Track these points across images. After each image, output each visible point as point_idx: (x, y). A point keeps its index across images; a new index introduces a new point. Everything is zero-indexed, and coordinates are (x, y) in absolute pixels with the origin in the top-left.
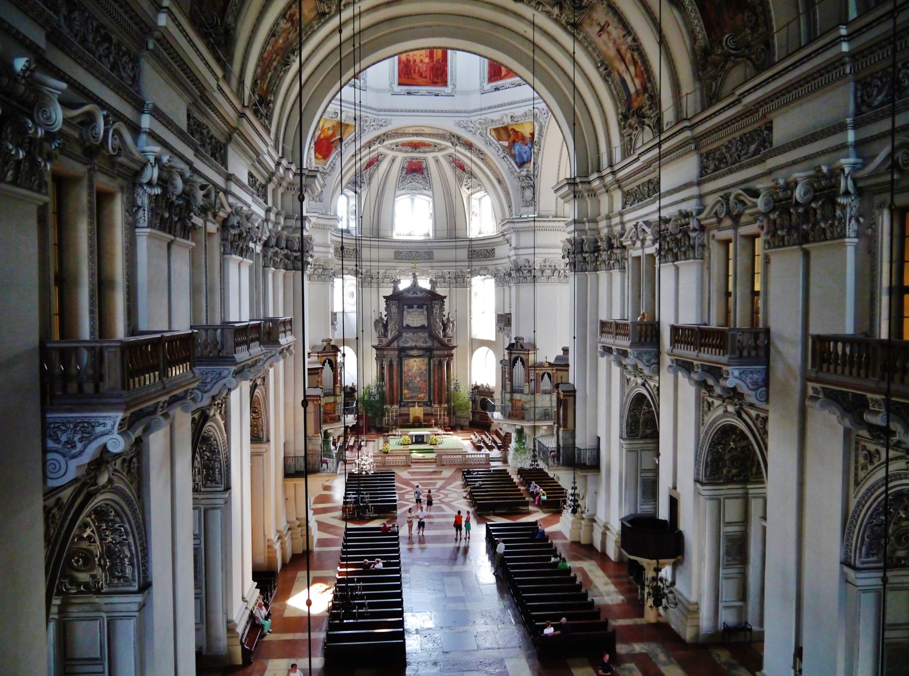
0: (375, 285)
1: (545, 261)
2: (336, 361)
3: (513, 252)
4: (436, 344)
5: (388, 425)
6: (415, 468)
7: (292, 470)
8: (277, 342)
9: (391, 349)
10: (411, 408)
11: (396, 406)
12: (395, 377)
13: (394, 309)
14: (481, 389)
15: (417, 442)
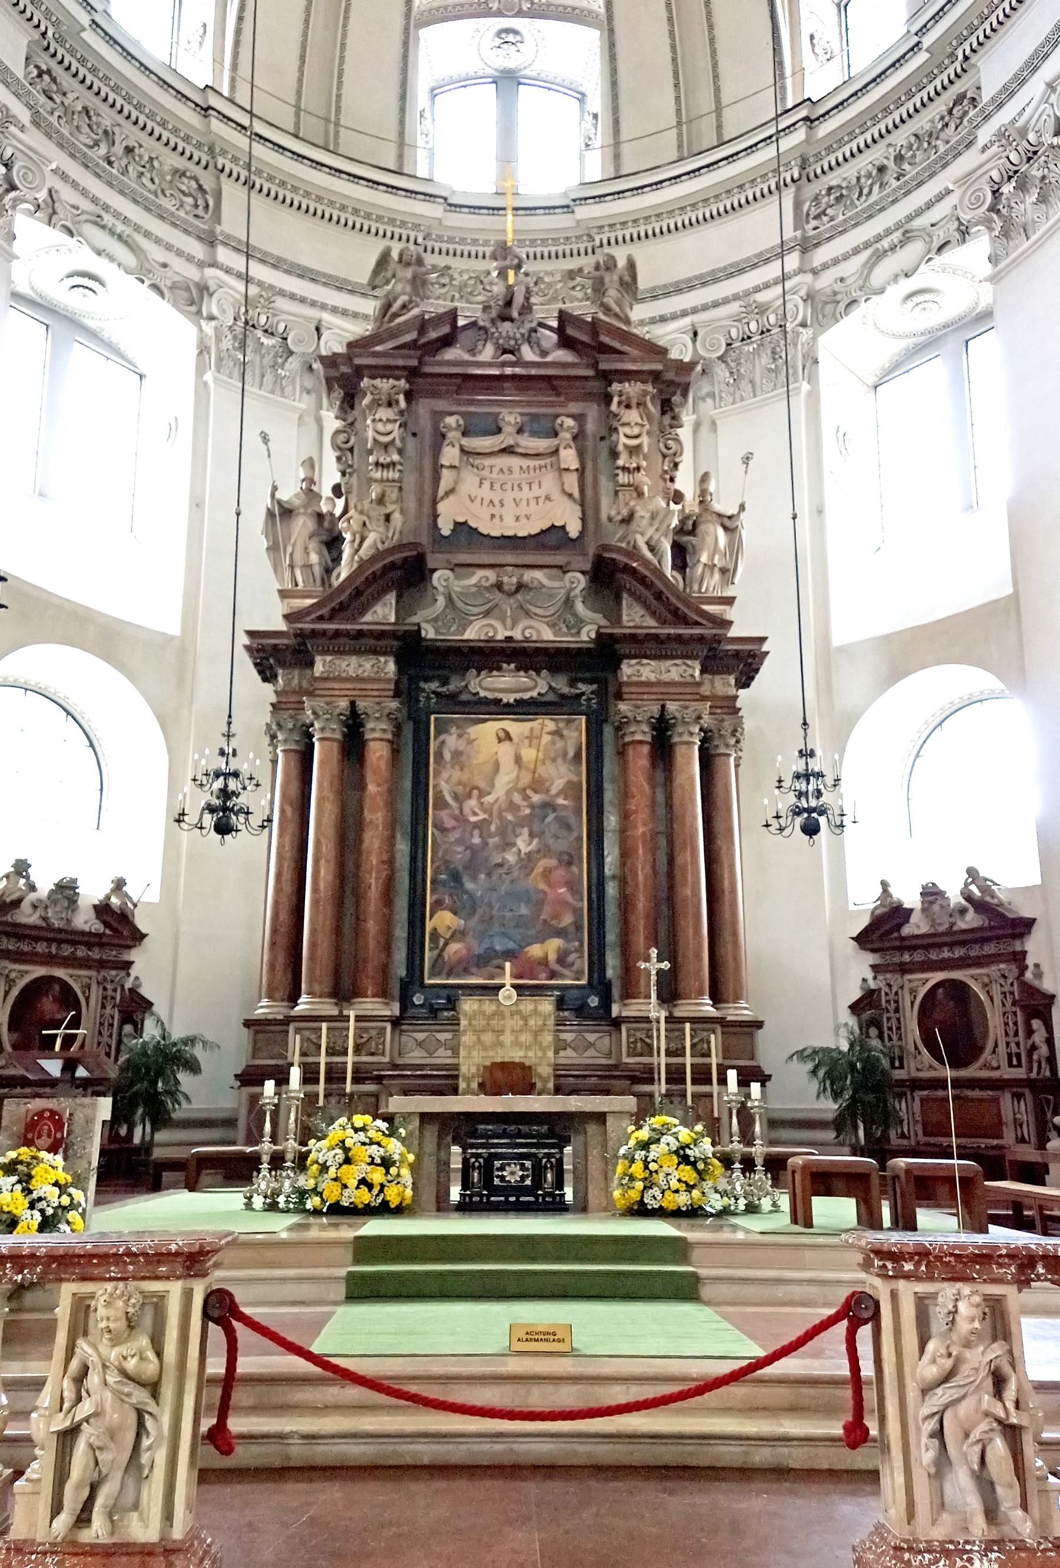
12: (375, 816)
14: (917, 926)
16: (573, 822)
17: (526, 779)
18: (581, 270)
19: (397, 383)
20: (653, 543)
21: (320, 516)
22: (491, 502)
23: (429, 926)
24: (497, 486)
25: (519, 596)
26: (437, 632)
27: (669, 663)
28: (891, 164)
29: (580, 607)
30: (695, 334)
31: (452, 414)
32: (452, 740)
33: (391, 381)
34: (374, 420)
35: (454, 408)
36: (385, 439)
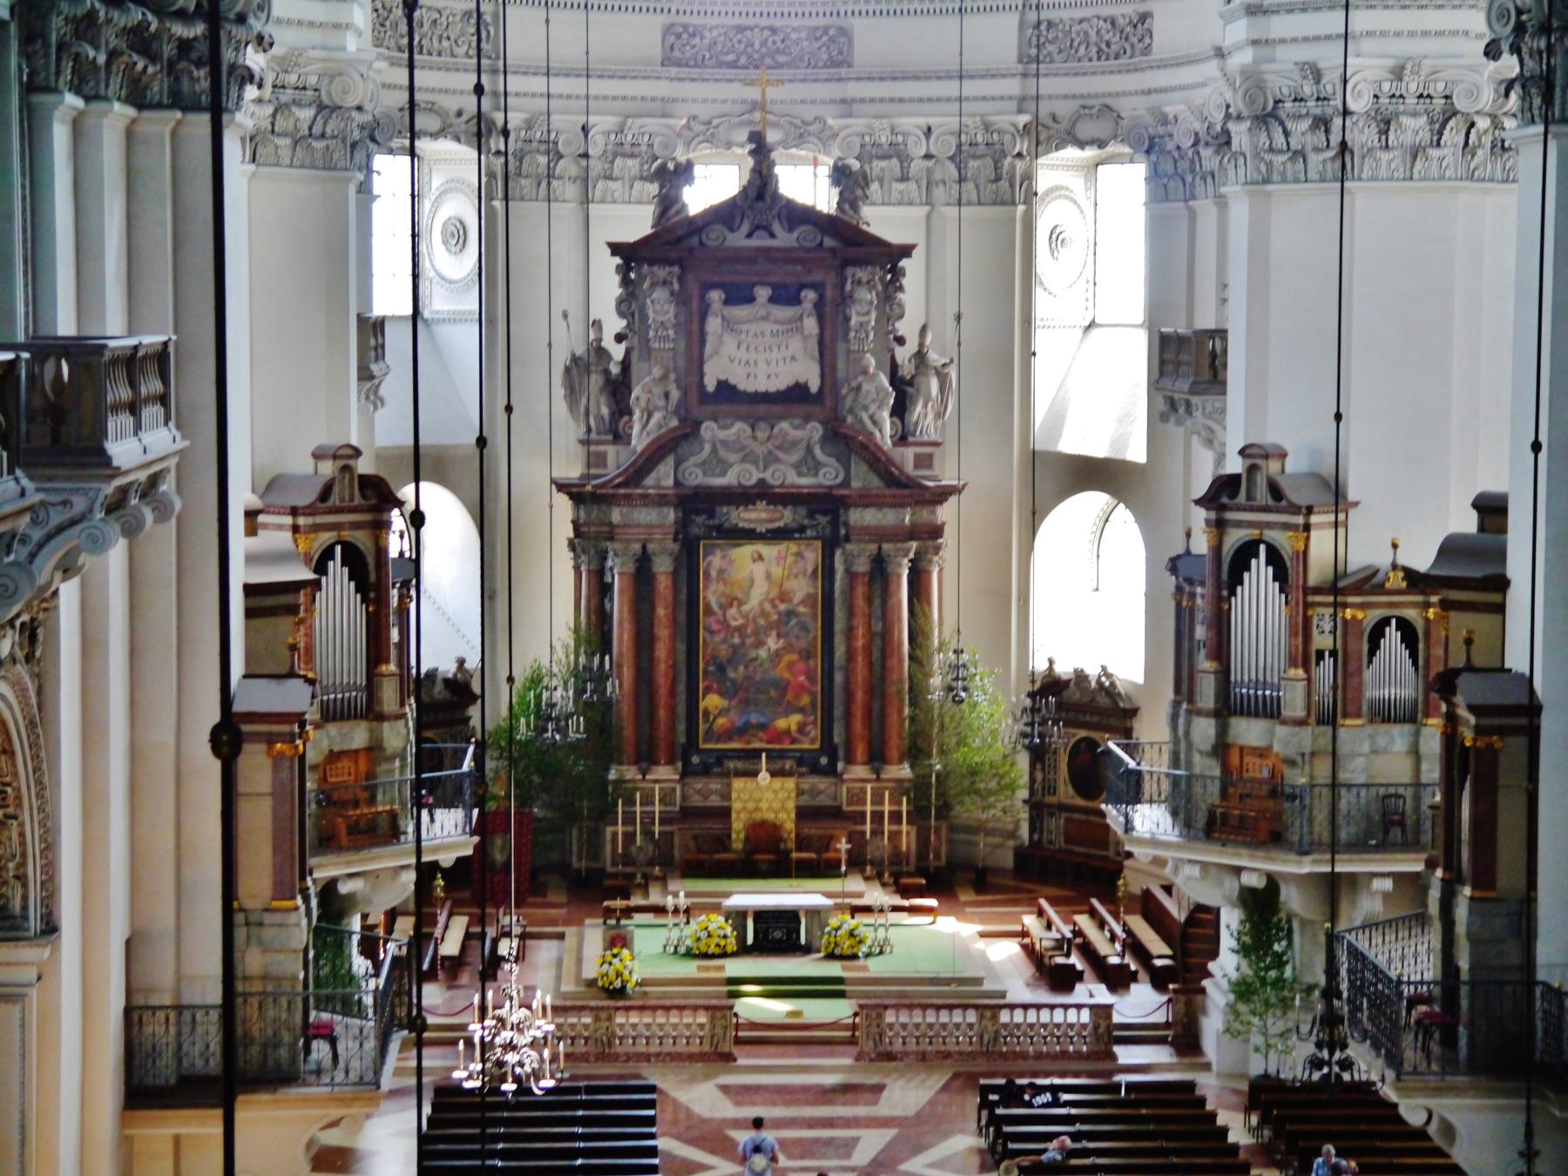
0: (568, 191)
1: (1398, 73)
2: (381, 551)
3: (1240, 30)
4: (862, 478)
5: (627, 859)
6: (754, 1069)
7: (165, 1071)
8: (96, 459)
9: (646, 500)
10: (738, 784)
11: (664, 773)
12: (663, 632)
13: (660, 306)
14: (1073, 694)
15: (764, 947)
16: (810, 625)
17: (774, 593)
18: (826, 30)
19: (672, 269)
20: (876, 418)
21: (607, 372)
22: (747, 362)
23: (702, 705)
24: (752, 348)
25: (770, 445)
26: (705, 474)
27: (886, 510)
28: (1093, 33)
29: (818, 452)
30: (929, 129)
31: (715, 286)
32: (716, 561)
33: (667, 269)
34: (653, 302)
35: (716, 279)
36: (660, 319)
